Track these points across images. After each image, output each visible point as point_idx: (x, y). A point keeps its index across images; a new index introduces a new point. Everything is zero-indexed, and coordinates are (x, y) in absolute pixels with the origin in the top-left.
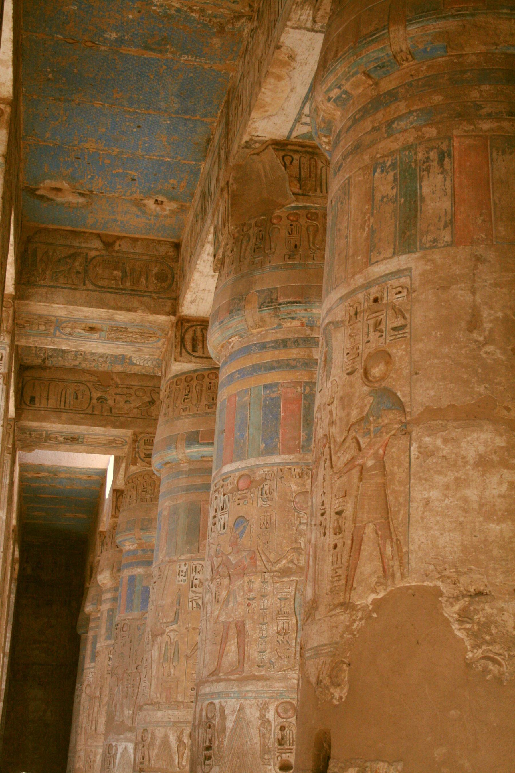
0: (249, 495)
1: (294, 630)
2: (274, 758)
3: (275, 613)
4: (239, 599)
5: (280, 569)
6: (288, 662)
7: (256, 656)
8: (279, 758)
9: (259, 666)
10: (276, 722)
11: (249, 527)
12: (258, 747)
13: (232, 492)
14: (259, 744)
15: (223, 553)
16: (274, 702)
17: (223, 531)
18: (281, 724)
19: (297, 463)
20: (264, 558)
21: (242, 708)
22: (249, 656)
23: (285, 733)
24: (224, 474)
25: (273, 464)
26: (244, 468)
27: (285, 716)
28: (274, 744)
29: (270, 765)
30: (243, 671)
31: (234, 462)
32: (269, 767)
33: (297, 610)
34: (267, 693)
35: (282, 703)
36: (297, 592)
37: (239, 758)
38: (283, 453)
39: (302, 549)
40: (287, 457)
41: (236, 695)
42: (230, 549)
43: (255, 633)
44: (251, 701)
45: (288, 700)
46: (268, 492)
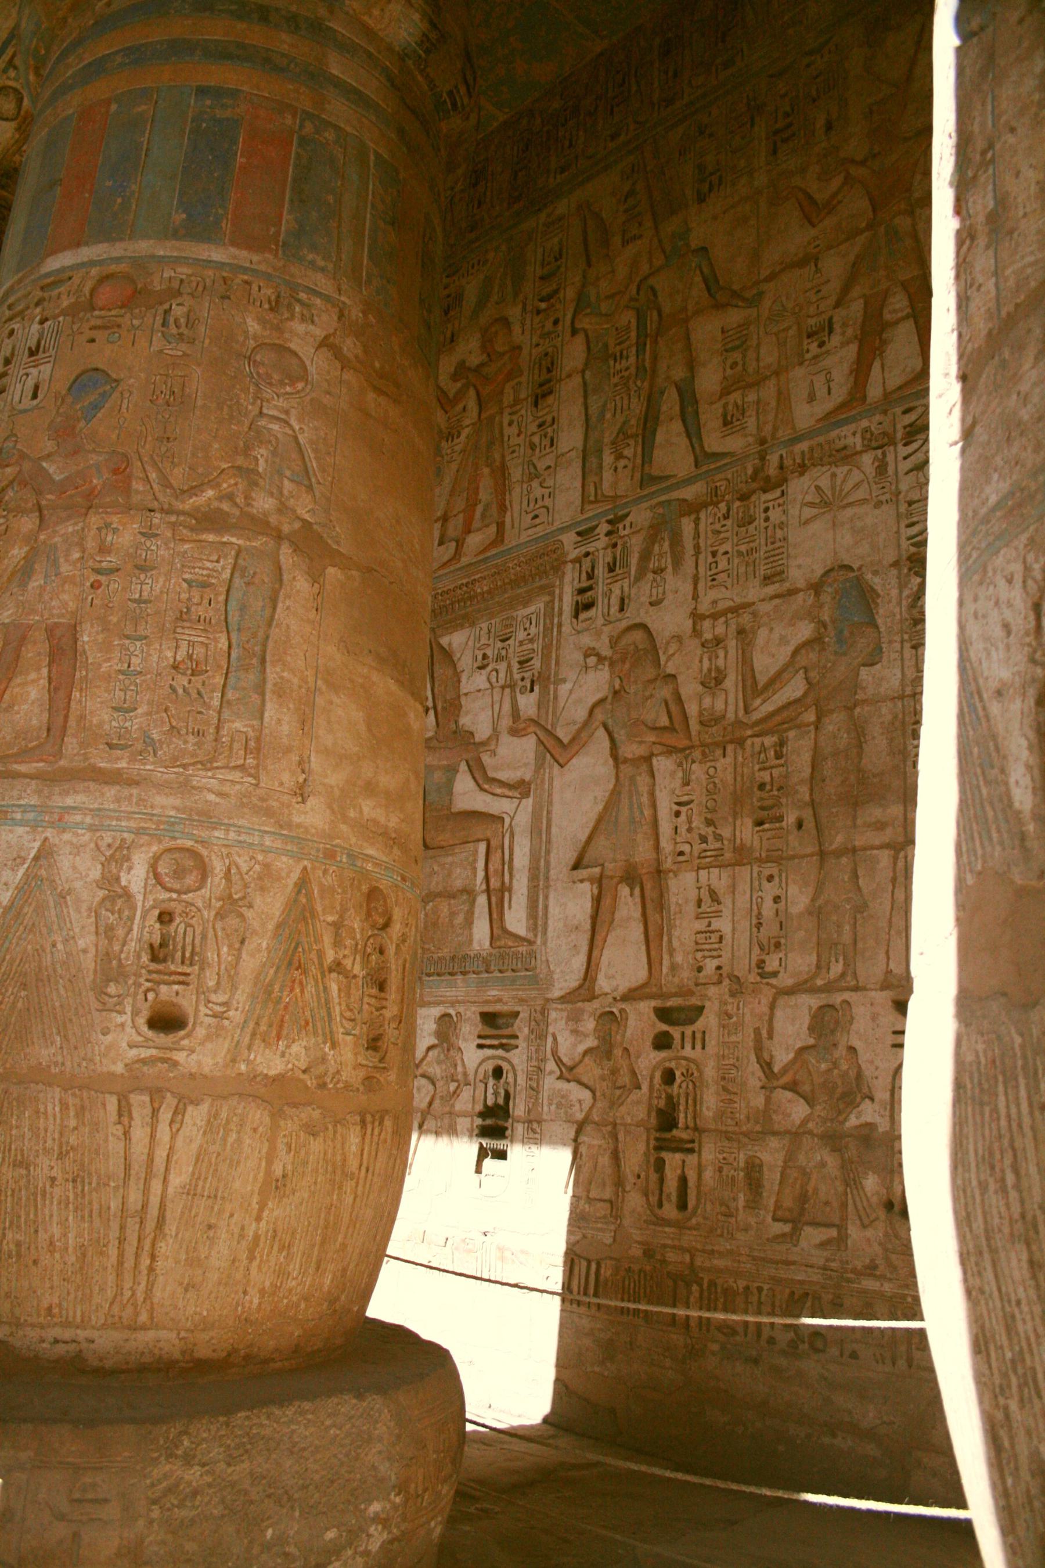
0: (126, 321)
1: (219, 667)
2: (136, 994)
3: (170, 616)
4: (65, 568)
5: (197, 509)
6: (199, 745)
7: (106, 717)
8: (151, 996)
9: (110, 746)
10: (151, 898)
11: (116, 395)
12: (89, 962)
13: (72, 312)
14: (91, 955)
15: (23, 456)
16: (149, 844)
17: (28, 403)
18: (165, 906)
19: (268, 277)
20: (153, 476)
21: (45, 853)
22: (82, 717)
23: (172, 928)
24: (48, 275)
25: (208, 263)
26: (118, 260)
27: (177, 886)
28: (139, 957)
29: (122, 1012)
30: (59, 754)
31: (87, 244)
32: (120, 1019)
33: (234, 618)
34: (129, 819)
35: (169, 850)
36: (237, 575)
37: (24, 986)
38: (234, 244)
39: (258, 474)
40: (244, 254)
41: (31, 816)
42: (50, 446)
43: (109, 660)
44: (77, 835)
45: (189, 843)
46: (183, 321)
